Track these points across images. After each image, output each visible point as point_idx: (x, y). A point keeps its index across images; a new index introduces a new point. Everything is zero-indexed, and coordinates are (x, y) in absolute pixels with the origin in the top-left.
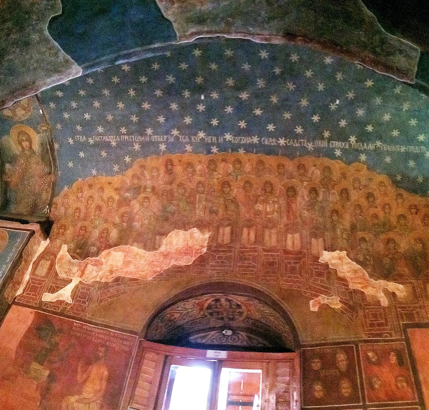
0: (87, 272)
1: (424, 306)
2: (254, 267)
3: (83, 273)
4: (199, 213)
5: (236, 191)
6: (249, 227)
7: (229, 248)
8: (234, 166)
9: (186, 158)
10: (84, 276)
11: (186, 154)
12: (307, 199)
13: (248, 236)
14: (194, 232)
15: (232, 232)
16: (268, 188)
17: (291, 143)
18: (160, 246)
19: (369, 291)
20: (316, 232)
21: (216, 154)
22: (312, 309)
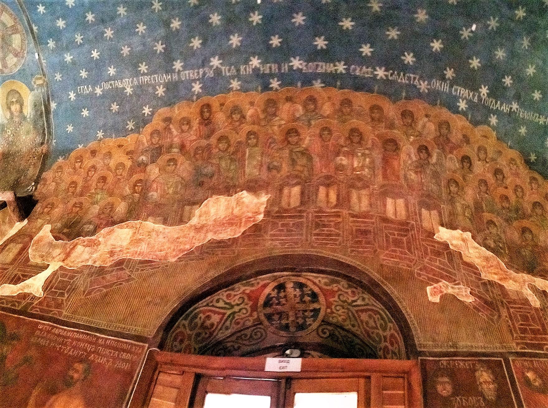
0: (74, 254)
2: (338, 235)
3: (68, 255)
4: (251, 169)
5: (308, 139)
6: (328, 186)
7: (299, 213)
8: (305, 107)
9: (231, 98)
10: (69, 259)
11: (231, 93)
12: (414, 159)
13: (326, 197)
14: (243, 196)
15: (302, 193)
16: (355, 137)
18: (189, 219)
20: (428, 201)
21: (277, 90)
22: (430, 298)
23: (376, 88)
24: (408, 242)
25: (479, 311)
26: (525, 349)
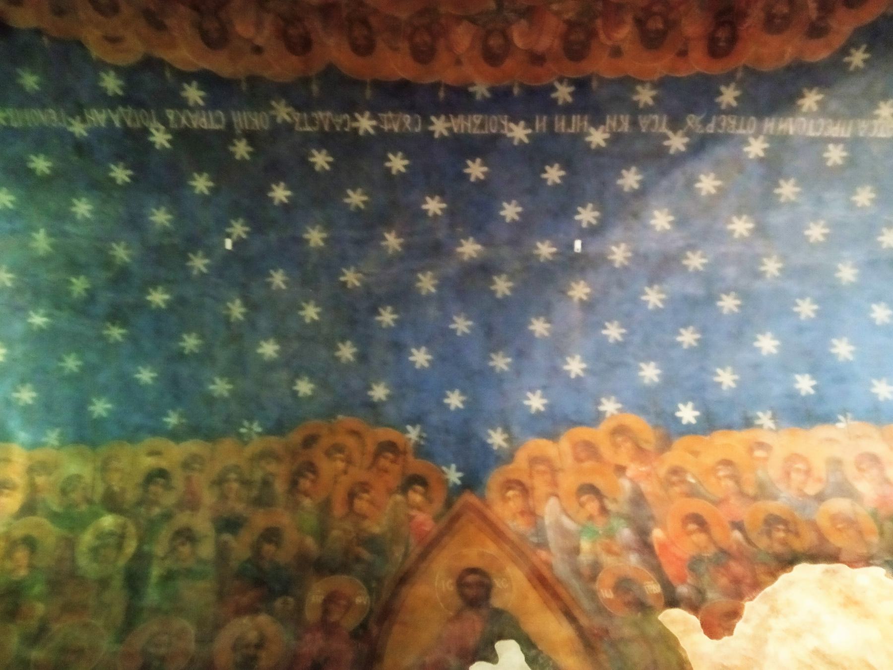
11: (656, 77)
17: (339, 120)
21: (561, 80)
23: (368, 93)
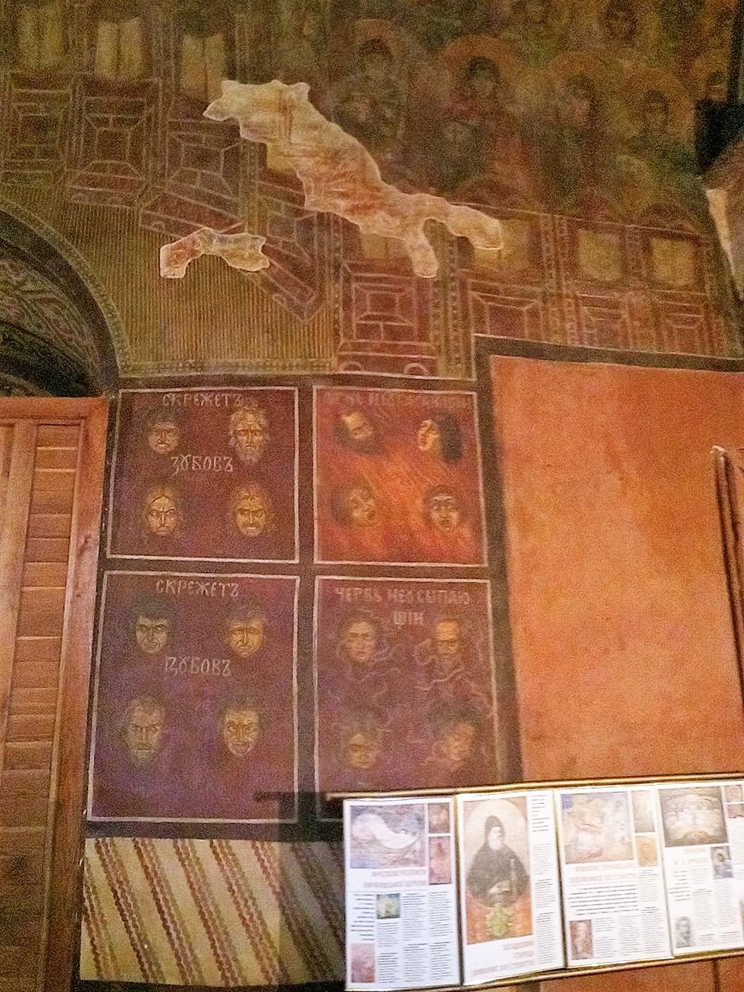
1: (560, 296)
19: (374, 226)
24: (137, 140)
25: (276, 289)
26: (357, 368)
